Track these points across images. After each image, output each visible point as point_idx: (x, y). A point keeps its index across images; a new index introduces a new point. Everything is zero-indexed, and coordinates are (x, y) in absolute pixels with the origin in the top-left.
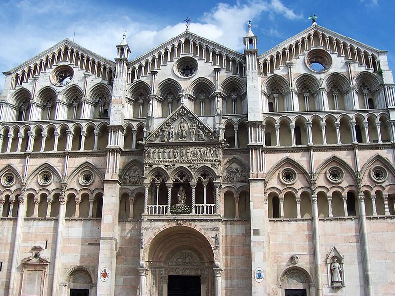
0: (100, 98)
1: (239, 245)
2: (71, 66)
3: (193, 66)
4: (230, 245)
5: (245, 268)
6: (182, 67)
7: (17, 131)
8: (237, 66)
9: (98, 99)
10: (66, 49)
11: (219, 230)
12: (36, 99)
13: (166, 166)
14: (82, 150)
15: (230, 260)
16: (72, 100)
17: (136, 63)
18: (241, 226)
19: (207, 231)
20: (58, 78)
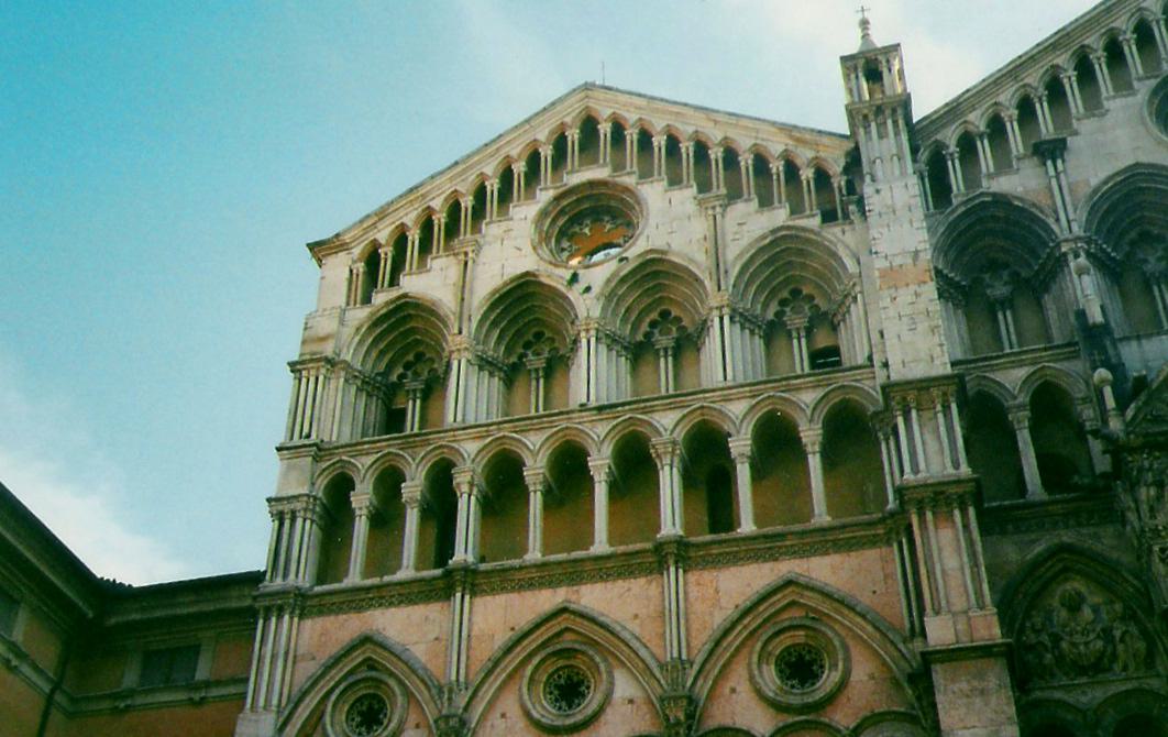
0: (783, 303)
2: (629, 180)
7: (390, 481)
9: (774, 308)
10: (589, 125)
12: (461, 343)
14: (747, 526)
16: (645, 327)
17: (944, 126)
20: (565, 244)
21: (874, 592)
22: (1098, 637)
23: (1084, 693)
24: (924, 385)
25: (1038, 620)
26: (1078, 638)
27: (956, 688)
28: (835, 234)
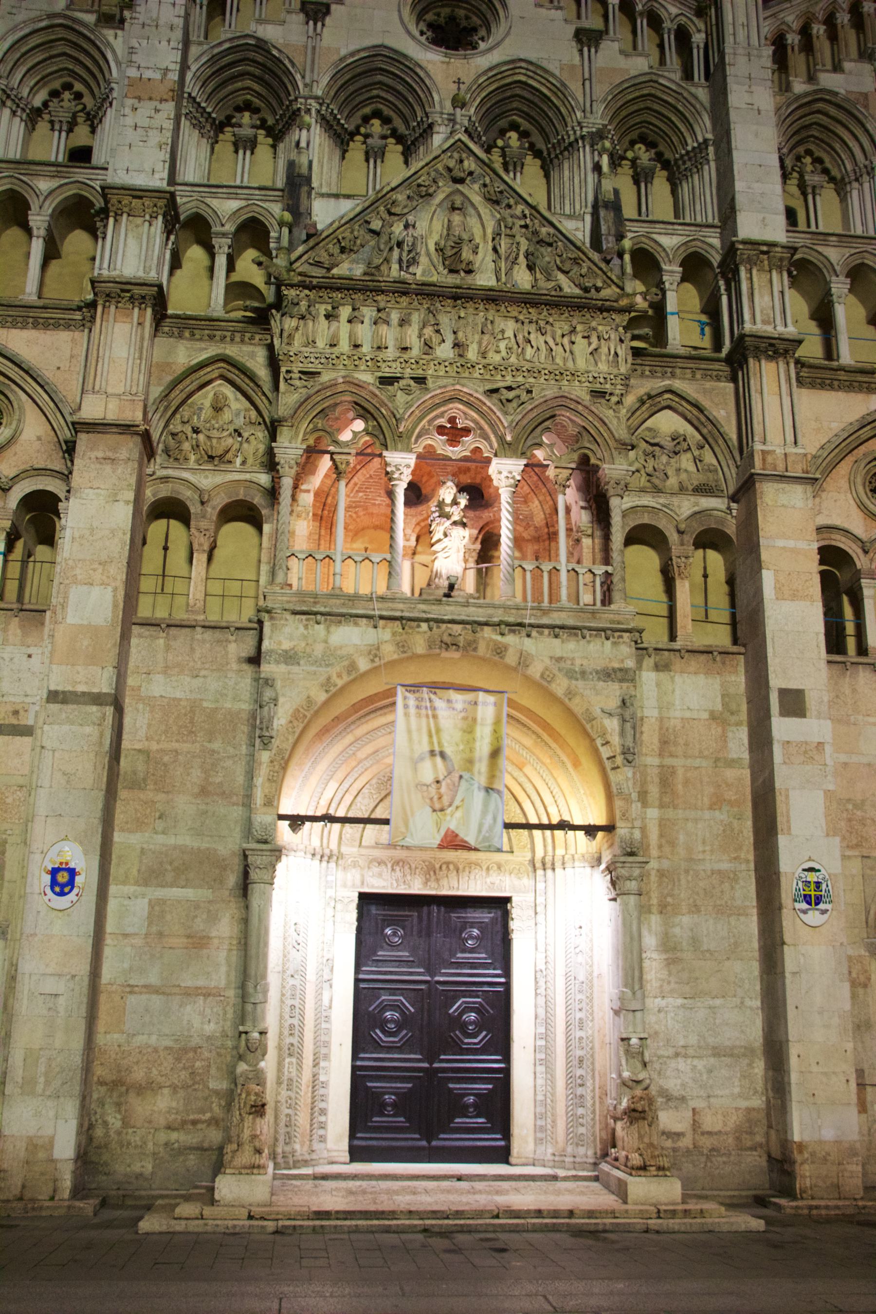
1: (697, 762)
3: (476, 20)
4: (656, 761)
5: (725, 866)
6: (430, 17)
8: (670, 40)
11: (633, 680)
13: (387, 381)
15: (660, 825)
18: (701, 679)
19: (580, 684)
21: (59, 368)
22: (230, 435)
23: (206, 477)
24: (138, 193)
25: (185, 412)
26: (215, 434)
27: (93, 455)
28: (109, 34)
